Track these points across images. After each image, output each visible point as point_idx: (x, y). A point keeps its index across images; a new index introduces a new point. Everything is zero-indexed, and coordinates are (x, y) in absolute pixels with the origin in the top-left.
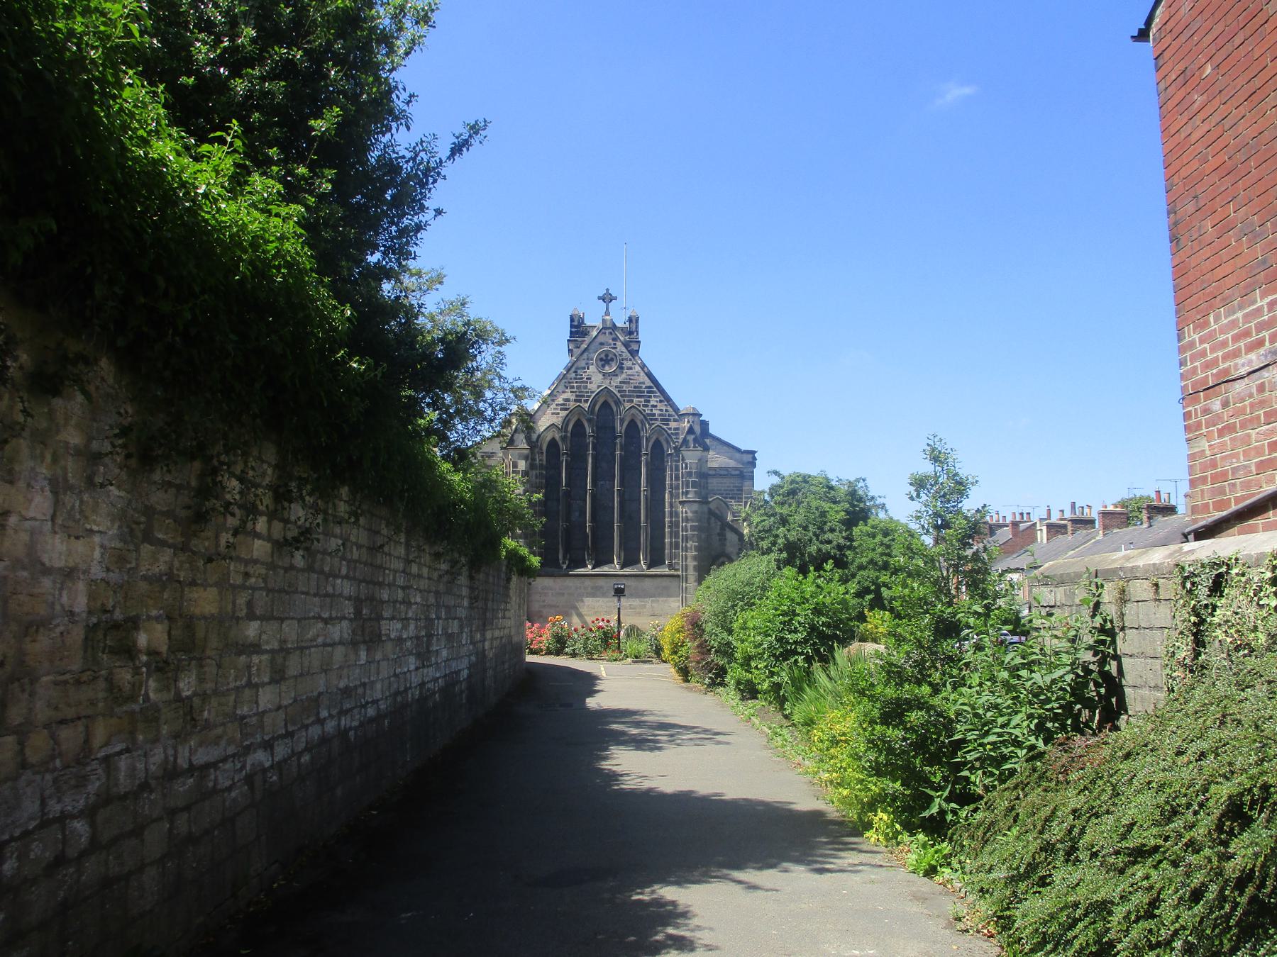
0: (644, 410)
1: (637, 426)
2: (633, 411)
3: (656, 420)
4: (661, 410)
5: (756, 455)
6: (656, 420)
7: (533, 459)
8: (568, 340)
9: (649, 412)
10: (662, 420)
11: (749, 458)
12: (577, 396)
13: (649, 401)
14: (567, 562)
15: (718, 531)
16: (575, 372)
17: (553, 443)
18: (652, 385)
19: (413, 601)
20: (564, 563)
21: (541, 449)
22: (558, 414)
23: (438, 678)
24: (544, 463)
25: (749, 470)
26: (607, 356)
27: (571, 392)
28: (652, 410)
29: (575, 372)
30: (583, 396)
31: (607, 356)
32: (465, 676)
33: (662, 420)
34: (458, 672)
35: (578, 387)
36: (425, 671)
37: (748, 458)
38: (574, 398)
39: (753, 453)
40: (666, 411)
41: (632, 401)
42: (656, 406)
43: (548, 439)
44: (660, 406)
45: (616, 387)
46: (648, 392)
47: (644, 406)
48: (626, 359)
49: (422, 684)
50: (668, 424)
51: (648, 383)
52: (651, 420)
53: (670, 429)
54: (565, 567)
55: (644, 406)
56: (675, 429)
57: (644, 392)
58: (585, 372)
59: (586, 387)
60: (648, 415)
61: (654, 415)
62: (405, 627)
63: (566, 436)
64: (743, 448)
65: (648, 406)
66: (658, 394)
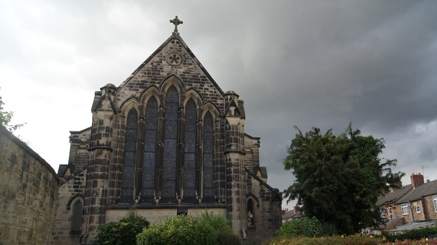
0: (200, 92)
2: (192, 91)
3: (208, 98)
4: (211, 92)
5: (260, 140)
6: (208, 98)
9: (203, 93)
10: (212, 98)
11: (255, 142)
12: (152, 79)
13: (203, 86)
14: (139, 198)
16: (152, 64)
17: (133, 112)
18: (205, 75)
20: (137, 198)
21: (123, 114)
22: (138, 90)
24: (126, 125)
25: (257, 149)
26: (175, 56)
27: (148, 76)
28: (205, 92)
29: (152, 64)
30: (157, 80)
31: (175, 56)
33: (212, 98)
35: (154, 74)
37: (255, 142)
38: (150, 80)
39: (258, 139)
40: (215, 92)
41: (191, 85)
42: (208, 89)
43: (130, 107)
44: (210, 89)
45: (180, 75)
46: (202, 80)
47: (199, 88)
48: (188, 59)
50: (216, 101)
51: (202, 74)
52: (204, 97)
53: (218, 104)
54: (137, 201)
55: (199, 88)
56: (221, 104)
57: (199, 80)
58: (159, 64)
59: (159, 74)
61: (207, 95)
63: (142, 106)
65: (202, 89)
66: (210, 81)
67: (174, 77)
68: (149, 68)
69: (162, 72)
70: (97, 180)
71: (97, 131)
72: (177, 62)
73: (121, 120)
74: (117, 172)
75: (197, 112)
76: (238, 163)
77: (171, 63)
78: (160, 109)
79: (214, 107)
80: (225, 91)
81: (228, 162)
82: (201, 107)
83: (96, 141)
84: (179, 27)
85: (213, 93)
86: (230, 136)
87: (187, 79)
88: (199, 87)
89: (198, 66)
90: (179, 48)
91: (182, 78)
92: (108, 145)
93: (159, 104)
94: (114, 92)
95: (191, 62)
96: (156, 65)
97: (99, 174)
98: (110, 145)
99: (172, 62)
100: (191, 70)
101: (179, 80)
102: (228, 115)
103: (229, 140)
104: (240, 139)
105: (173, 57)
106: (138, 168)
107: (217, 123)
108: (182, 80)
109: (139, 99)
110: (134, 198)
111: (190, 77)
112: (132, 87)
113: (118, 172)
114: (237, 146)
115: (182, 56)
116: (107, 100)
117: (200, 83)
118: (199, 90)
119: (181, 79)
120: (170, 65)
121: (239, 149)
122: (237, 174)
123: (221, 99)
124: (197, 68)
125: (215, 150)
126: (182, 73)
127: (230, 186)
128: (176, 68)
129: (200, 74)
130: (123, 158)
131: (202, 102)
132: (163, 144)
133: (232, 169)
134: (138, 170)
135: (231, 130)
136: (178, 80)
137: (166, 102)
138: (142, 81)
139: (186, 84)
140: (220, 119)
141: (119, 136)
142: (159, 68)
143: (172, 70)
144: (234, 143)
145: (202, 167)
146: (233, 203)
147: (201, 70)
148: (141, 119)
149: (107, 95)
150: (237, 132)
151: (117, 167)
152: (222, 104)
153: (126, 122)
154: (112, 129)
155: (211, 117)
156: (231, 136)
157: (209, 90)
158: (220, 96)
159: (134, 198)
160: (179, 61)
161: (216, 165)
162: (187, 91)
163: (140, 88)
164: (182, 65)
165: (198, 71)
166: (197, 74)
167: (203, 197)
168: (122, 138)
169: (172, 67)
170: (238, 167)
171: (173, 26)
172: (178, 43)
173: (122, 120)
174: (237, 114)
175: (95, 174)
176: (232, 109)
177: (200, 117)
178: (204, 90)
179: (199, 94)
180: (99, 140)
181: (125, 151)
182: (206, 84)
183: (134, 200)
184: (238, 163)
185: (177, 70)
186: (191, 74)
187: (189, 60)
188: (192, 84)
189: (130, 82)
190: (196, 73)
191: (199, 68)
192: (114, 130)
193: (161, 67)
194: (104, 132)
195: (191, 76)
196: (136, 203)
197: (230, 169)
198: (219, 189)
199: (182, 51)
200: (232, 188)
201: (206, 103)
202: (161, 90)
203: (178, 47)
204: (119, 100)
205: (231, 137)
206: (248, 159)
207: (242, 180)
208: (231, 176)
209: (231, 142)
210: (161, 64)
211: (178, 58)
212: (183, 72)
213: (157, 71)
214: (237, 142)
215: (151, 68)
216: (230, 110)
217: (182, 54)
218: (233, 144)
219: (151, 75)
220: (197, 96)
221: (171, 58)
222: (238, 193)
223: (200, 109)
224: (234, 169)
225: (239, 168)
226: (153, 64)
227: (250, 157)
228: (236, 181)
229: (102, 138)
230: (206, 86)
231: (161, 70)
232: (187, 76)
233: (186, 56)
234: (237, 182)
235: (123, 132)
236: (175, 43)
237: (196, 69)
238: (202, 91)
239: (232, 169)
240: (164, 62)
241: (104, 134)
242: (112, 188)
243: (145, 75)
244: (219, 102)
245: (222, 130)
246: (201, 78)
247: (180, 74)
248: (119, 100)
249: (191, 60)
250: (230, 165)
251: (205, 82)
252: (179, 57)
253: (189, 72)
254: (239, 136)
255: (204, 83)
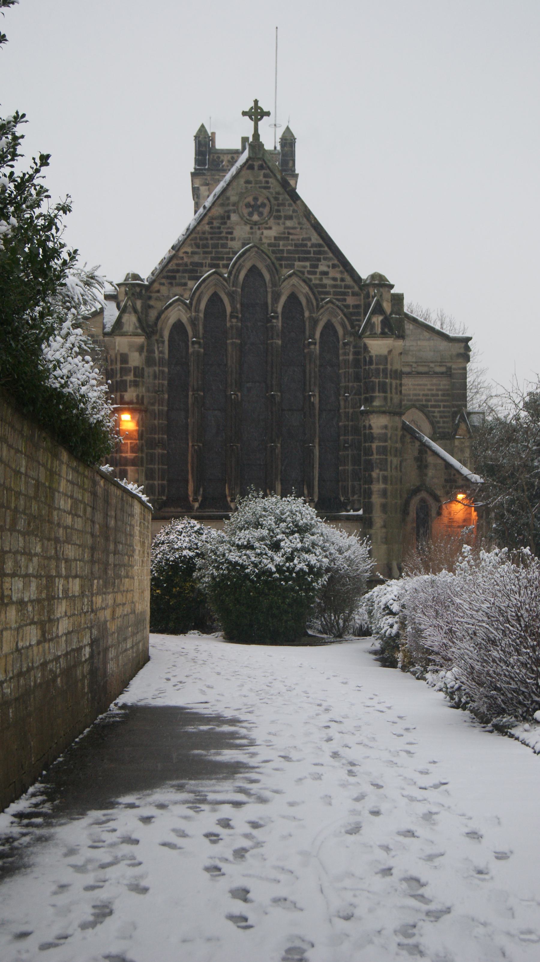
0: (310, 280)
1: (300, 303)
3: (328, 293)
4: (335, 279)
6: (328, 293)
7: (150, 351)
8: (193, 175)
9: (317, 282)
10: (335, 293)
12: (212, 259)
13: (317, 266)
14: (200, 499)
15: (416, 453)
16: (210, 223)
18: (321, 242)
19: (33, 552)
20: (195, 500)
21: (162, 336)
23: (59, 657)
24: (166, 356)
25: (461, 366)
26: (256, 199)
27: (205, 253)
28: (321, 279)
30: (222, 259)
31: (256, 199)
32: (87, 656)
33: (335, 293)
34: (79, 650)
36: (47, 645)
37: (458, 348)
38: (208, 261)
40: (342, 280)
42: (325, 273)
43: (172, 321)
45: (270, 245)
47: (309, 273)
48: (283, 205)
49: (44, 664)
50: (345, 300)
51: (315, 238)
52: (320, 293)
53: (347, 307)
54: (196, 505)
55: (309, 273)
57: (309, 252)
60: (316, 286)
61: (324, 286)
62: (26, 586)
63: (197, 318)
64: (451, 335)
65: (315, 273)
66: (331, 255)
67: (256, 249)
68: (204, 233)
69: (233, 239)
70: (126, 468)
71: (119, 376)
72: (260, 214)
73: (158, 348)
74: (159, 451)
75: (304, 322)
76: (386, 434)
77: (248, 217)
78: (230, 321)
79: (340, 312)
80: (364, 273)
81: (367, 431)
82: (314, 315)
83: (118, 394)
84: (263, 123)
85: (339, 283)
86: (371, 378)
87: (283, 253)
88: (308, 269)
89: (305, 220)
90: (264, 180)
91: (274, 252)
92: (140, 401)
93: (229, 309)
94: (141, 290)
95: (291, 213)
96: (218, 225)
97: (128, 457)
98: (142, 403)
99: (251, 214)
100: (291, 231)
101: (266, 257)
102: (368, 333)
103: (369, 388)
104: (391, 385)
105: (252, 203)
106: (195, 444)
107: (347, 347)
108: (273, 257)
109: (189, 305)
110: (191, 499)
111: (289, 248)
112: (174, 278)
113: (160, 451)
114: (385, 398)
115: (272, 200)
116: (130, 313)
117: (310, 261)
118: (310, 276)
119: (270, 254)
120: (246, 223)
121: (389, 404)
122: (384, 457)
123: (354, 294)
124: (304, 227)
125: (342, 403)
126: (273, 241)
127: (370, 481)
128: (259, 229)
129: (310, 239)
130: (166, 422)
131: (315, 303)
132: (239, 394)
133: (374, 446)
134: (196, 447)
135: (373, 367)
136: (265, 256)
137: (242, 305)
138: (192, 263)
139: (281, 265)
140: (352, 339)
141: (157, 382)
142: (225, 231)
143: (252, 233)
144: (379, 392)
145: (317, 440)
146: (374, 512)
147: (311, 228)
148: (196, 346)
149: (130, 303)
150: (386, 369)
151: (157, 442)
152: (357, 306)
153: (166, 351)
154: (143, 369)
155: (336, 332)
156: (373, 379)
157: (331, 275)
158: (353, 287)
159: (191, 499)
160: (266, 211)
161: (345, 436)
162: (284, 280)
163: (191, 279)
164: (271, 222)
165: (306, 234)
166: (303, 240)
167: (319, 498)
168: (163, 385)
169: (251, 228)
170: (386, 441)
171: (249, 124)
172: (261, 167)
173: (161, 349)
174: (386, 330)
175: (121, 457)
176: (377, 320)
177: (312, 336)
178: (318, 276)
179: (311, 288)
180: (123, 393)
181: (168, 410)
182: (323, 262)
183: (191, 502)
184: (386, 434)
185: (262, 234)
186: (292, 240)
187: (287, 208)
188: (294, 265)
189: (170, 267)
190: (301, 237)
191: (307, 225)
192: (146, 369)
193: (229, 228)
194: (130, 378)
195: (292, 246)
196: (195, 508)
197: (371, 446)
198: (350, 483)
199: (272, 186)
200: (374, 483)
201: (322, 307)
202: (231, 281)
203: (261, 178)
204: (150, 307)
205: (372, 381)
206: (441, 390)
207: (393, 467)
208: (371, 460)
209: (373, 391)
210: (228, 222)
211: (263, 205)
212: (275, 238)
213: (220, 238)
214: (385, 392)
215: (210, 233)
216: (372, 322)
217: (272, 193)
218: (375, 397)
219: (210, 250)
220: (306, 289)
221: (248, 205)
222: (384, 493)
223: (311, 318)
224: (377, 446)
225: (388, 444)
226: (212, 223)
227: (445, 385)
228: (381, 470)
229: (129, 390)
230: (322, 268)
231: (229, 236)
232: (284, 245)
233: (281, 199)
234: (384, 472)
235: (163, 372)
236: (256, 167)
237: (301, 228)
238: (316, 278)
239: (374, 446)
240: (234, 217)
241: (130, 381)
242: (151, 482)
243: (197, 250)
244: (350, 301)
245: (357, 363)
246: (312, 249)
247: (269, 242)
248: (150, 307)
249: (291, 208)
250: (371, 438)
251: (322, 256)
252: (266, 201)
253: (286, 235)
254: (391, 378)
255: (319, 260)
